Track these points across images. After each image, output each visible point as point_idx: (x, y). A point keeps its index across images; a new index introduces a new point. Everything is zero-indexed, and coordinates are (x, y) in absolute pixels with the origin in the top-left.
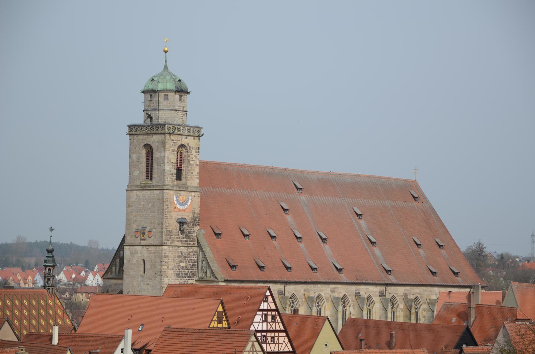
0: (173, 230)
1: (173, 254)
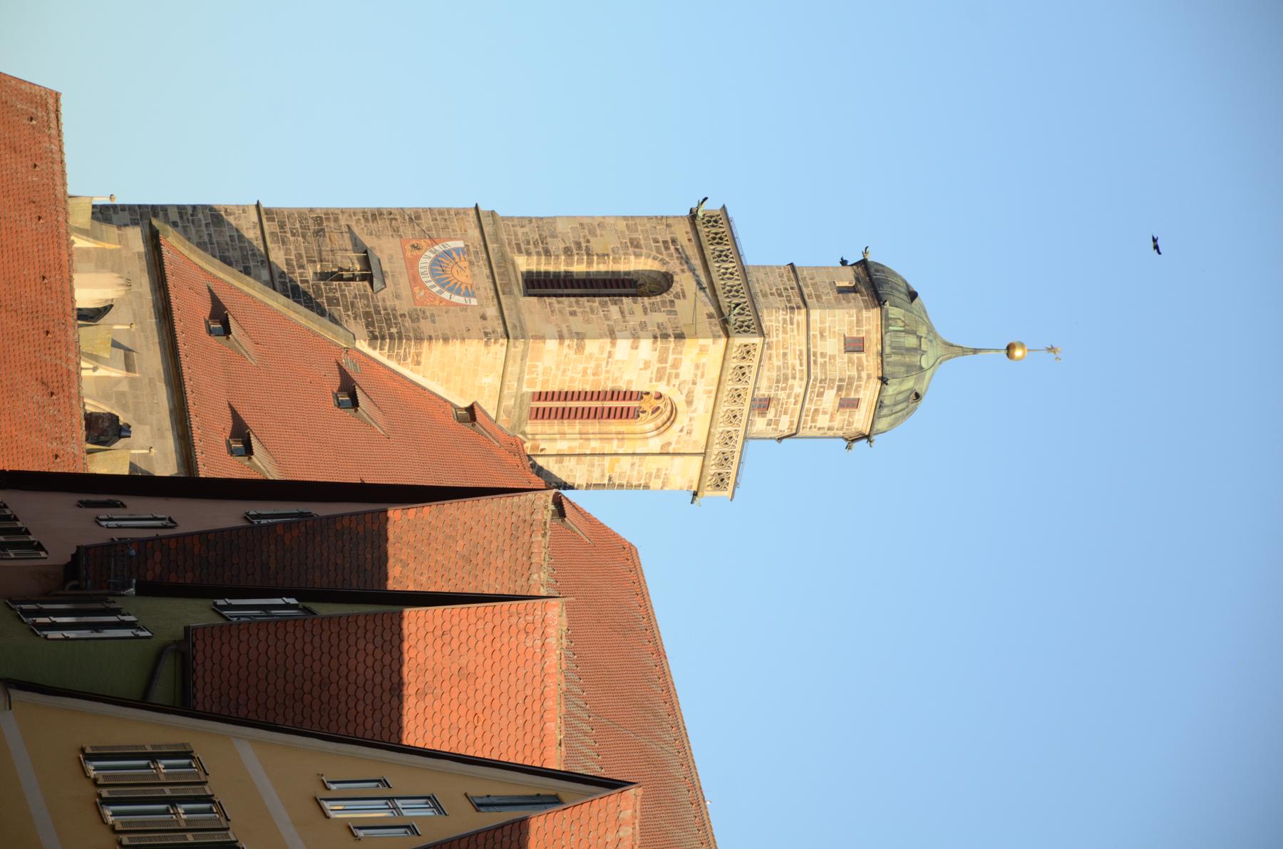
0: (328, 240)
1: (231, 241)
